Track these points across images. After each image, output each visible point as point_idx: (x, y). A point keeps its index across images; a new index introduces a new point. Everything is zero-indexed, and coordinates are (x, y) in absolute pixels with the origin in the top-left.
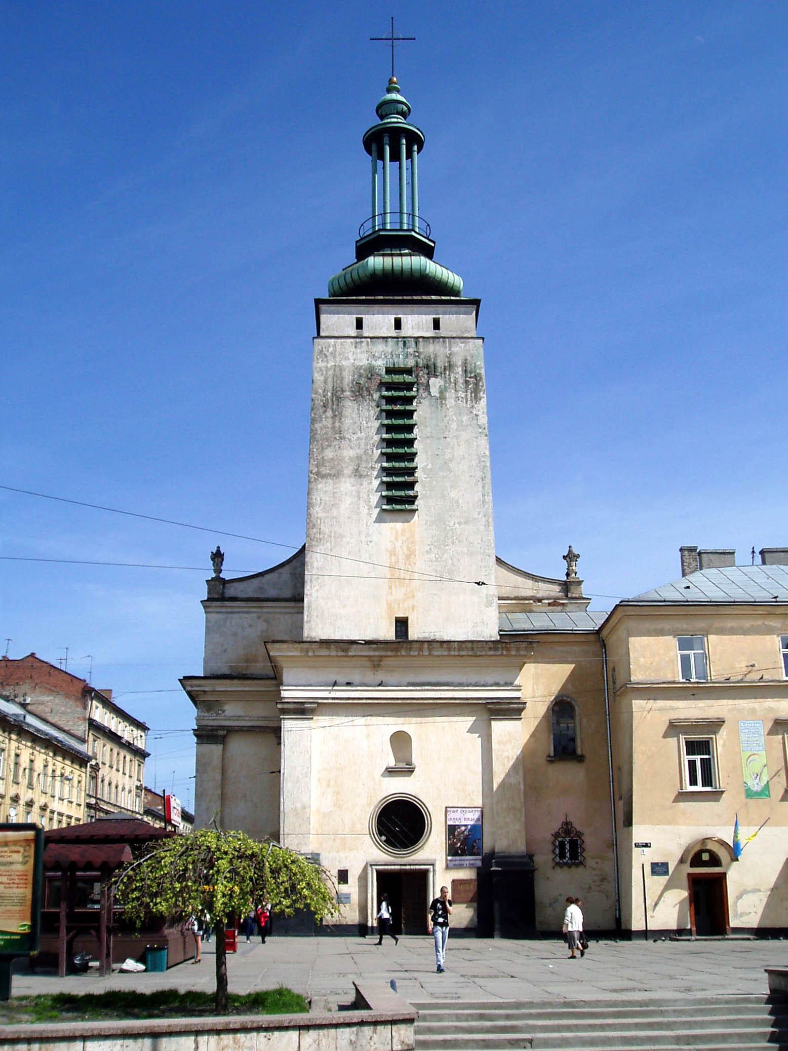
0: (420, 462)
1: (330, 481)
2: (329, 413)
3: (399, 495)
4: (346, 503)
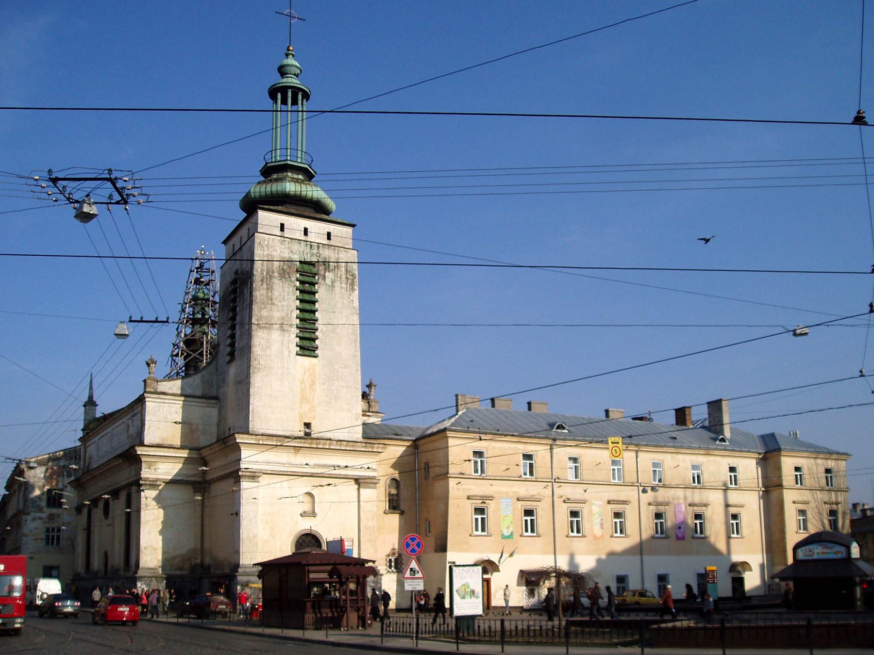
0: (318, 325)
1: (265, 331)
2: (265, 286)
3: (307, 345)
4: (275, 347)
